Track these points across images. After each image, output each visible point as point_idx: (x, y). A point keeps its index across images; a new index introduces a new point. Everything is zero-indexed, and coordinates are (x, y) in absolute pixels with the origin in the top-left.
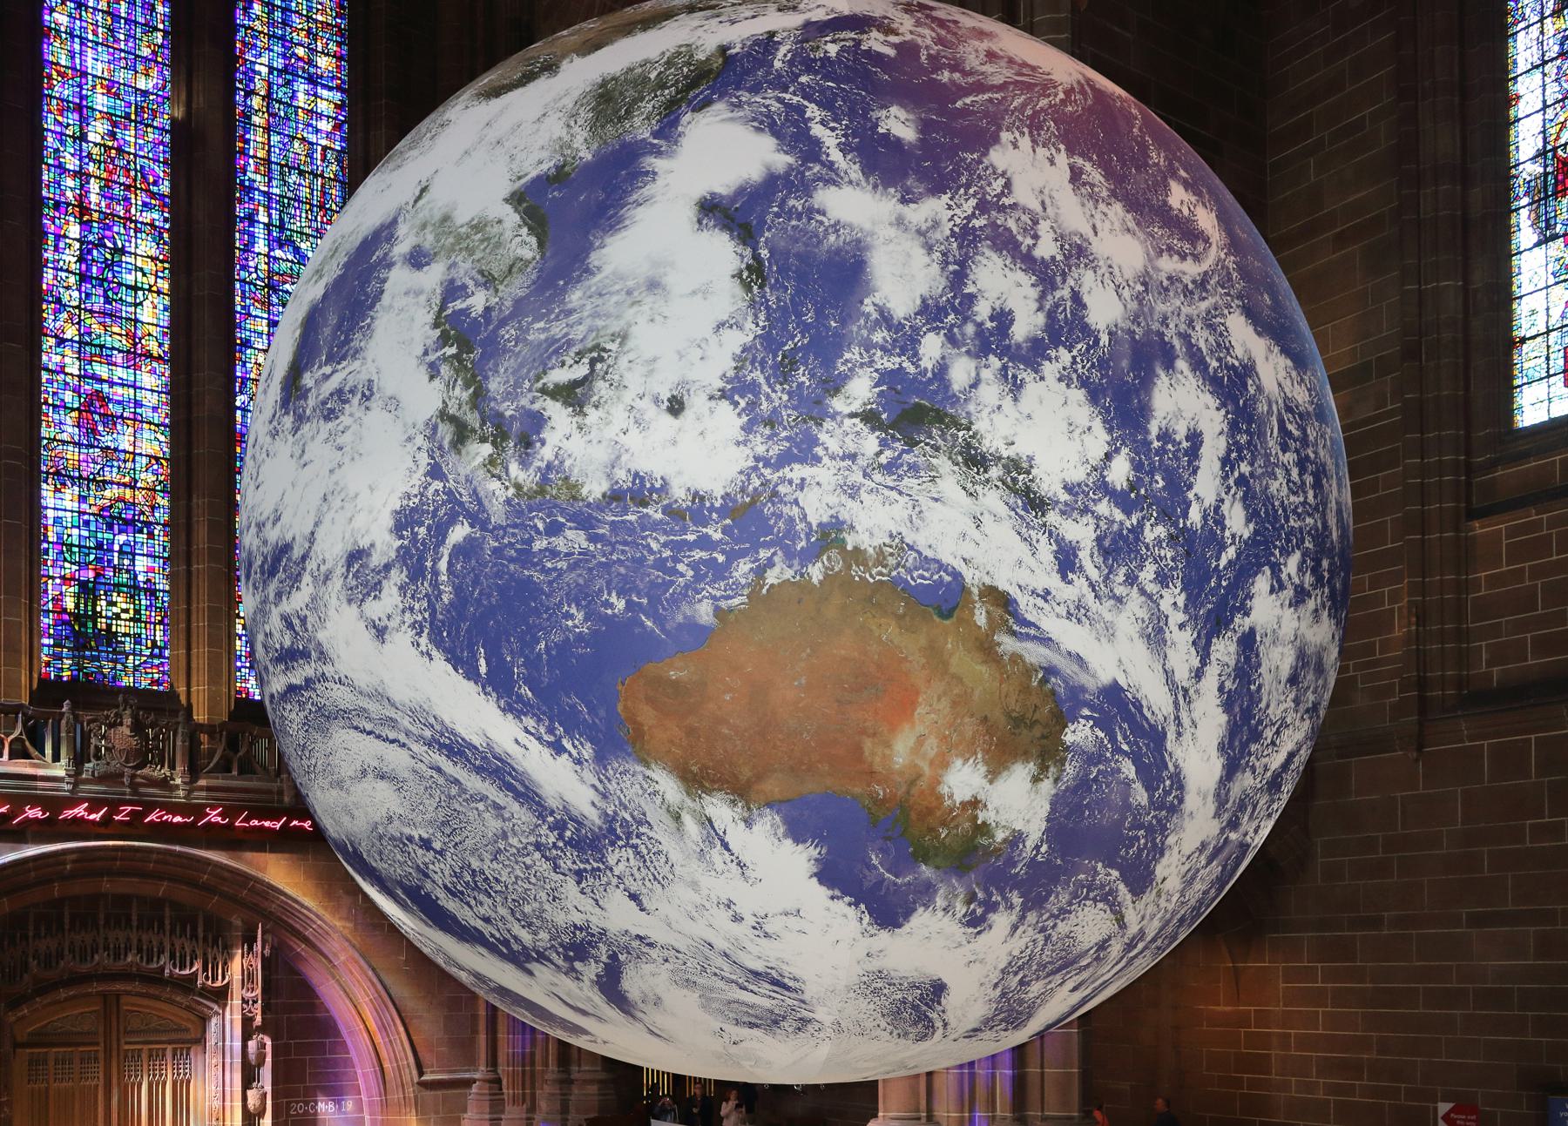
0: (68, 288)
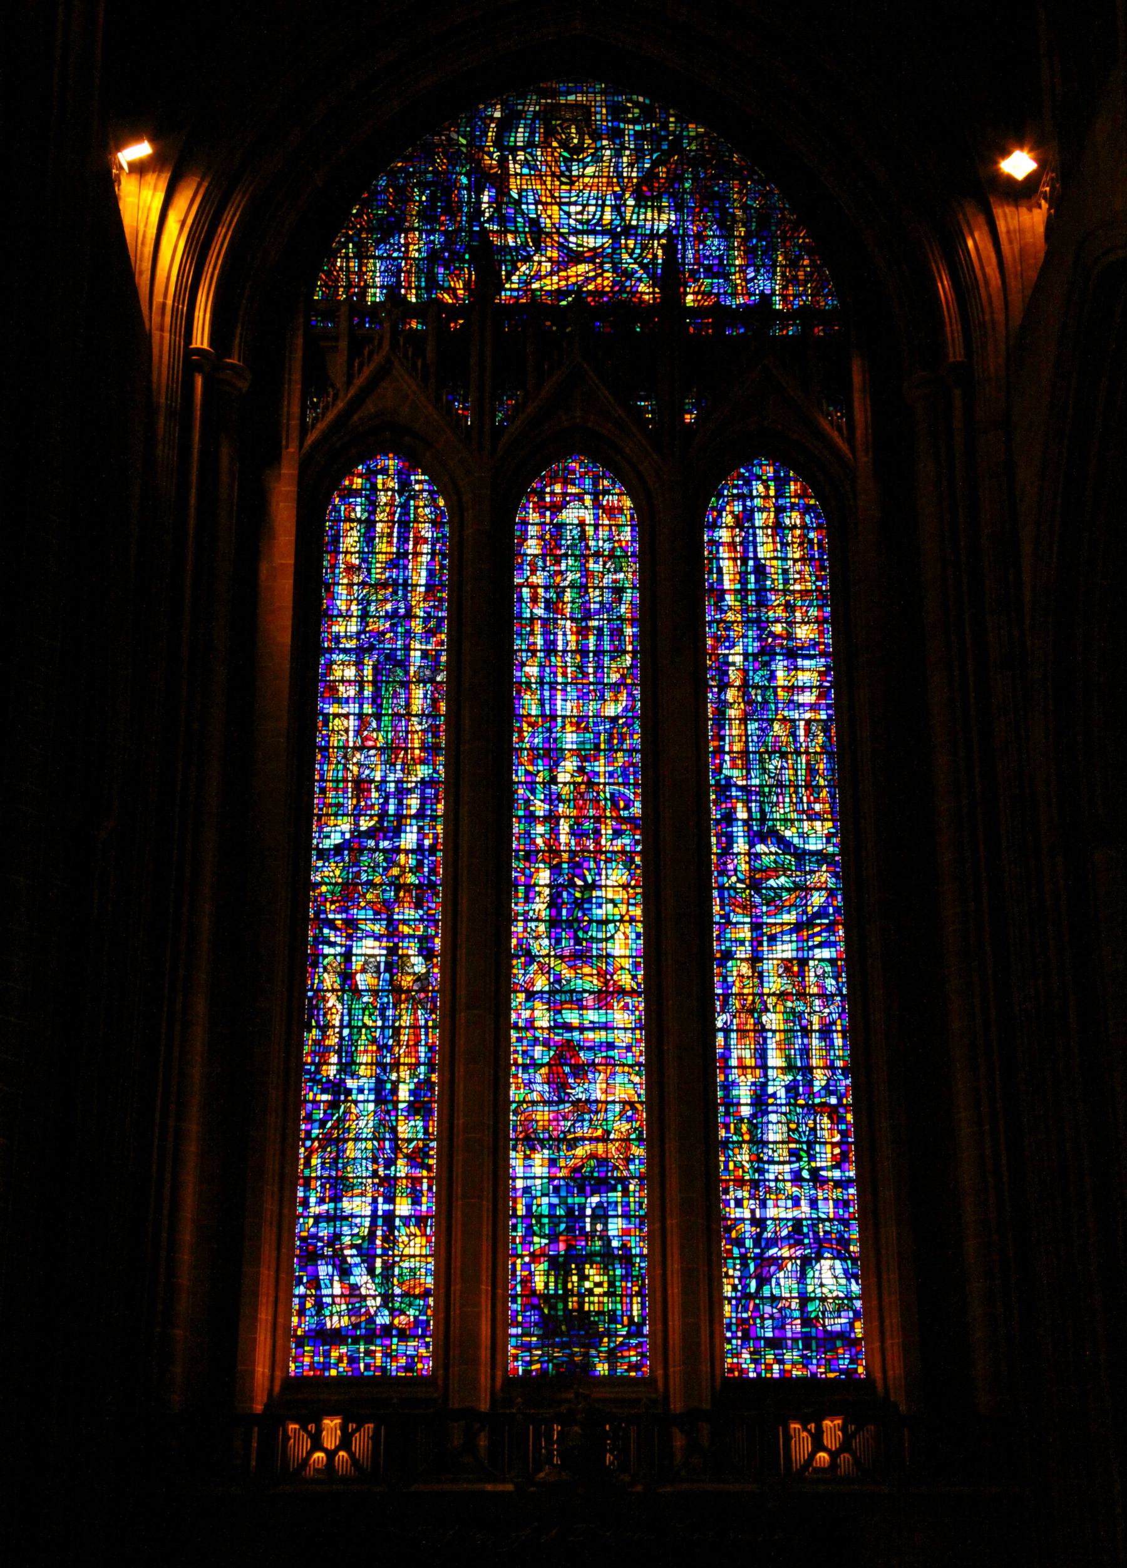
0: (537, 938)
